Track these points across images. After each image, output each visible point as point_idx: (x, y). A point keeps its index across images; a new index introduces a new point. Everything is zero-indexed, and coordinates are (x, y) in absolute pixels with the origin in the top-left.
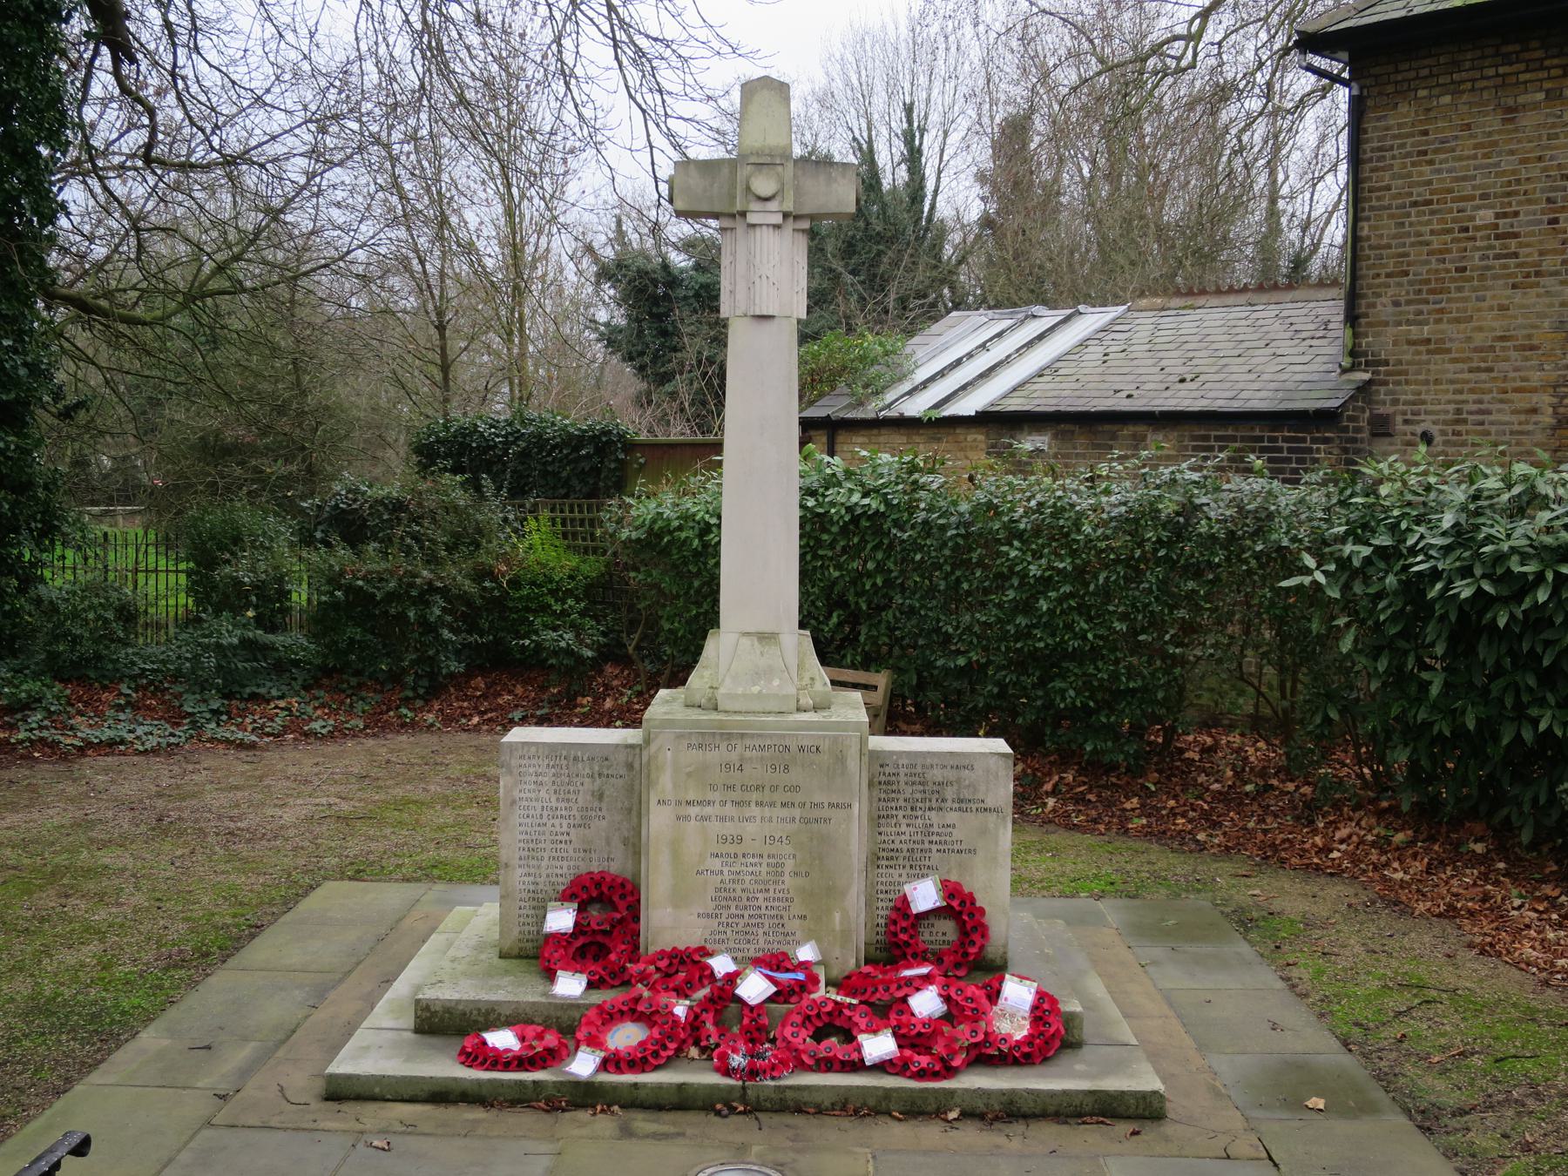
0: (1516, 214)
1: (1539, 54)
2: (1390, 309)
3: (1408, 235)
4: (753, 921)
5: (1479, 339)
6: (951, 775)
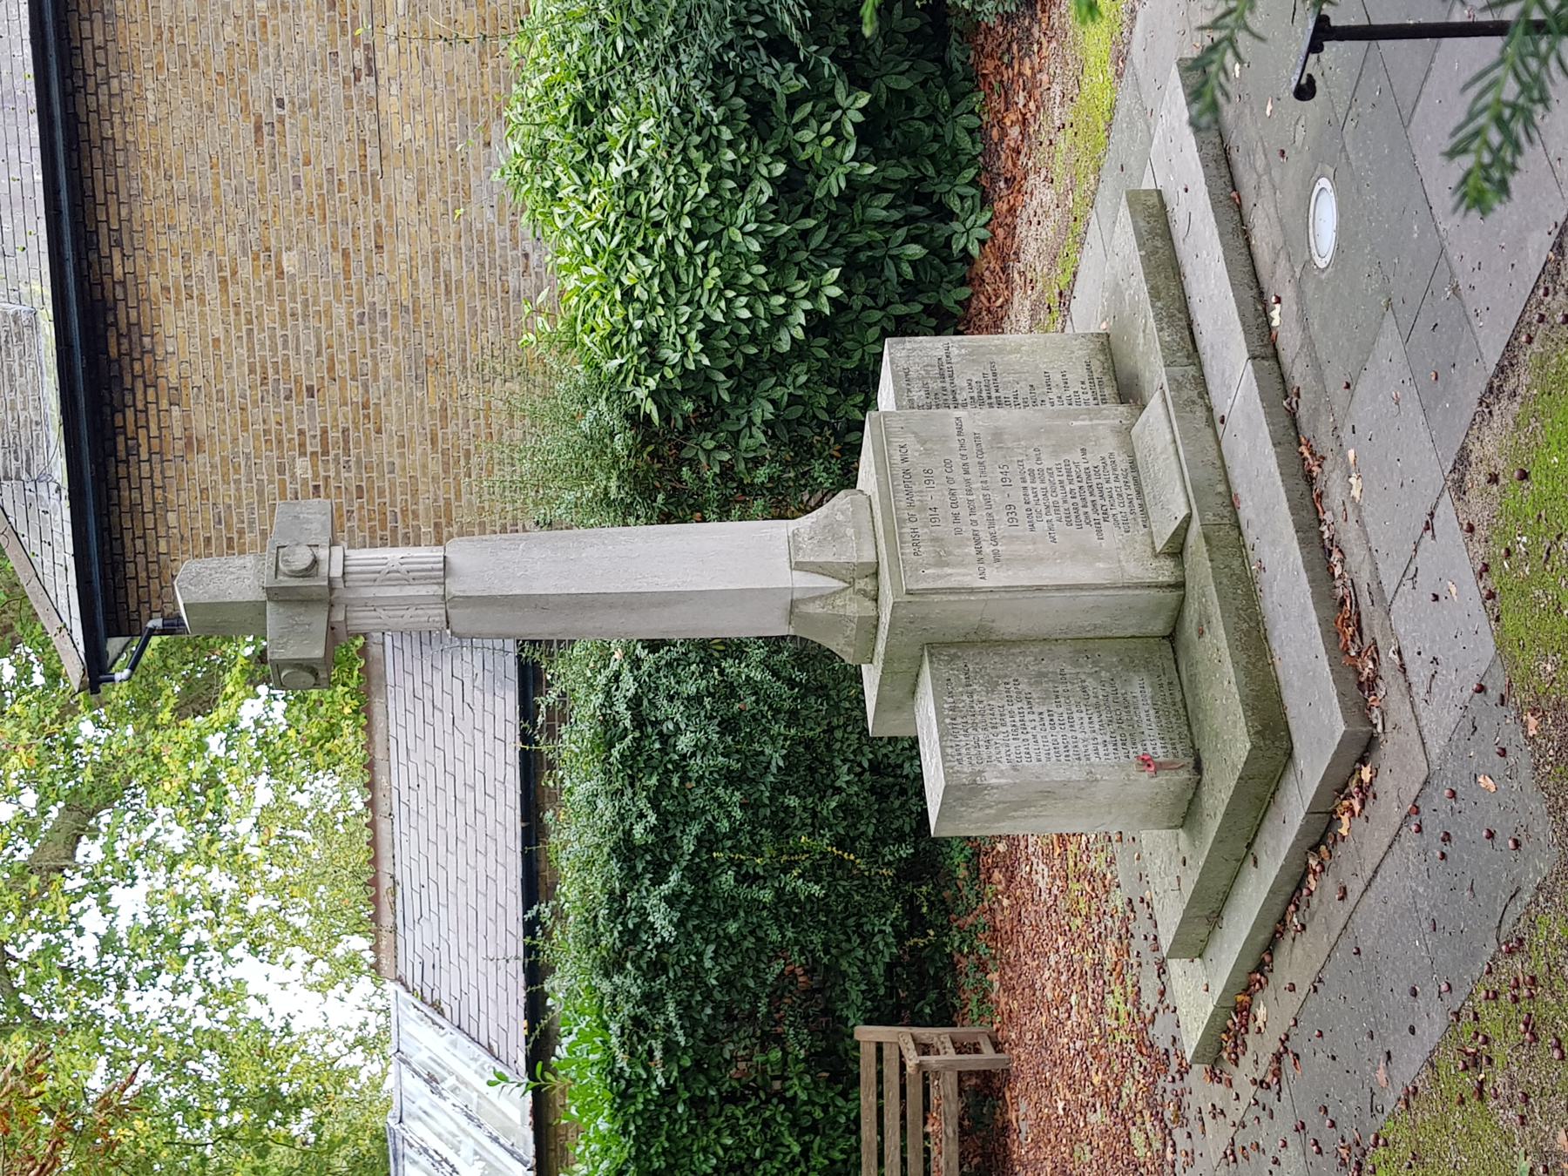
4: (1096, 492)
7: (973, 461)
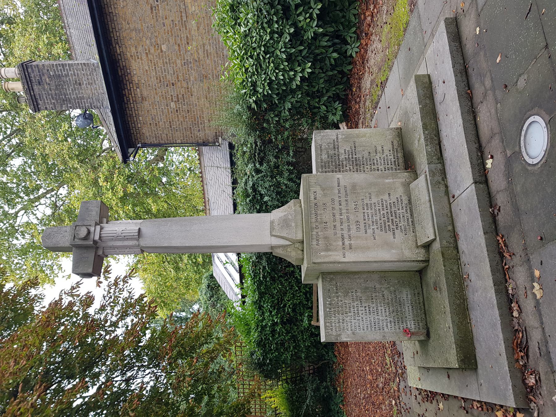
0: (171, 96)
1: (126, 90)
2: (200, 132)
3: (179, 128)
4: (394, 215)
5: (207, 105)
6: (324, 152)
7: (343, 199)
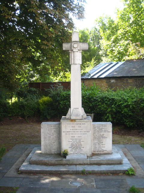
7: (82, 133)
